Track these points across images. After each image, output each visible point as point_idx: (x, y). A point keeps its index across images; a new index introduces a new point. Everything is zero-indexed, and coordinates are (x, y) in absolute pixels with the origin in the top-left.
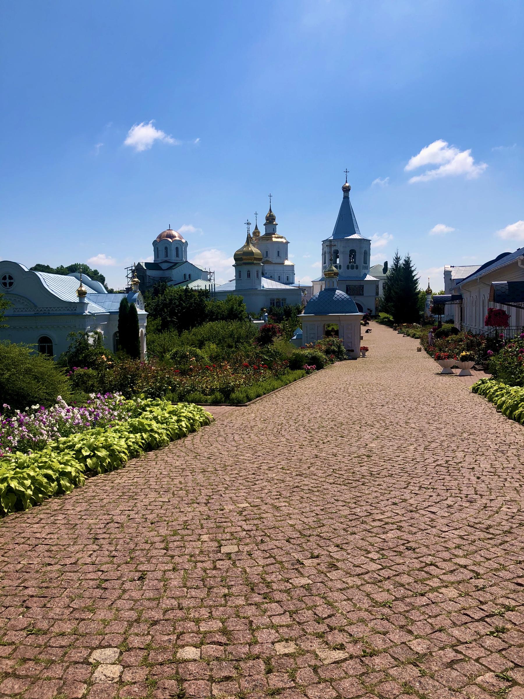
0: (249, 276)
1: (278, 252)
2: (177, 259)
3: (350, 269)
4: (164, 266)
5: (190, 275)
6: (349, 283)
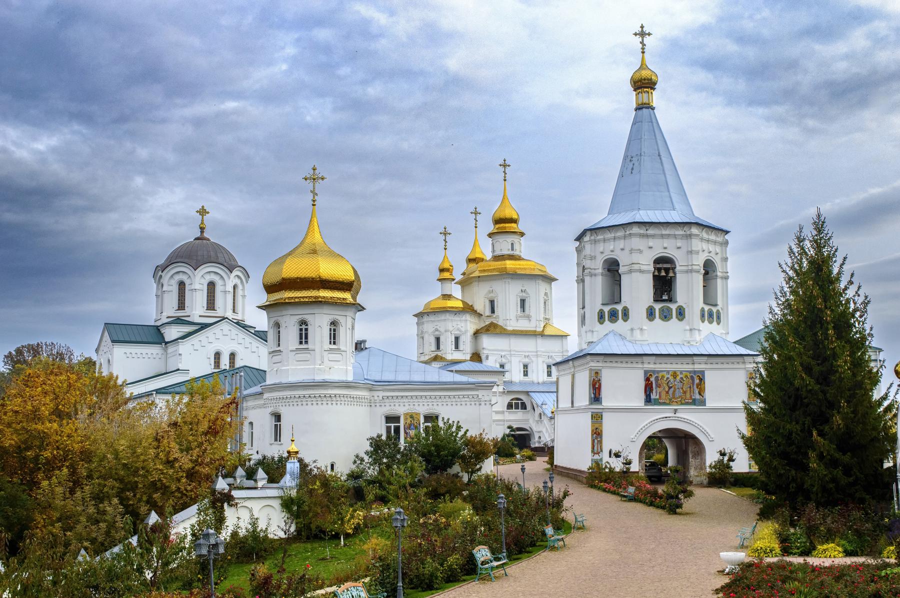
0: (304, 337)
1: (523, 302)
2: (211, 313)
3: (657, 320)
4: (171, 333)
5: (232, 356)
6: (650, 366)
